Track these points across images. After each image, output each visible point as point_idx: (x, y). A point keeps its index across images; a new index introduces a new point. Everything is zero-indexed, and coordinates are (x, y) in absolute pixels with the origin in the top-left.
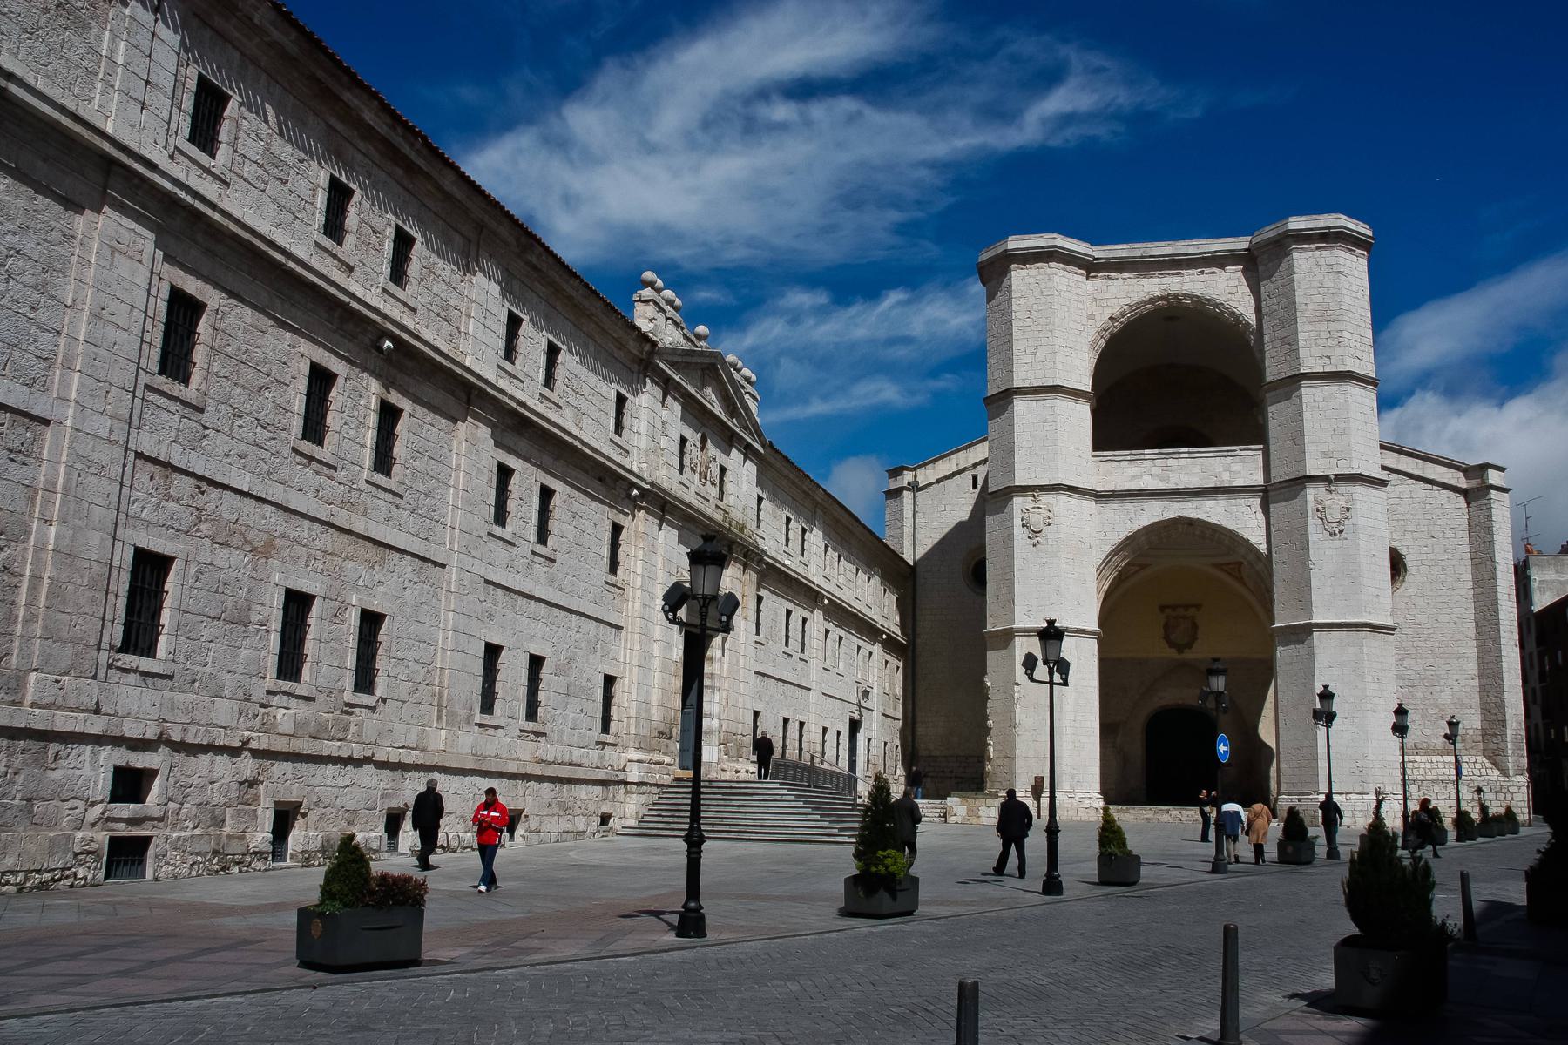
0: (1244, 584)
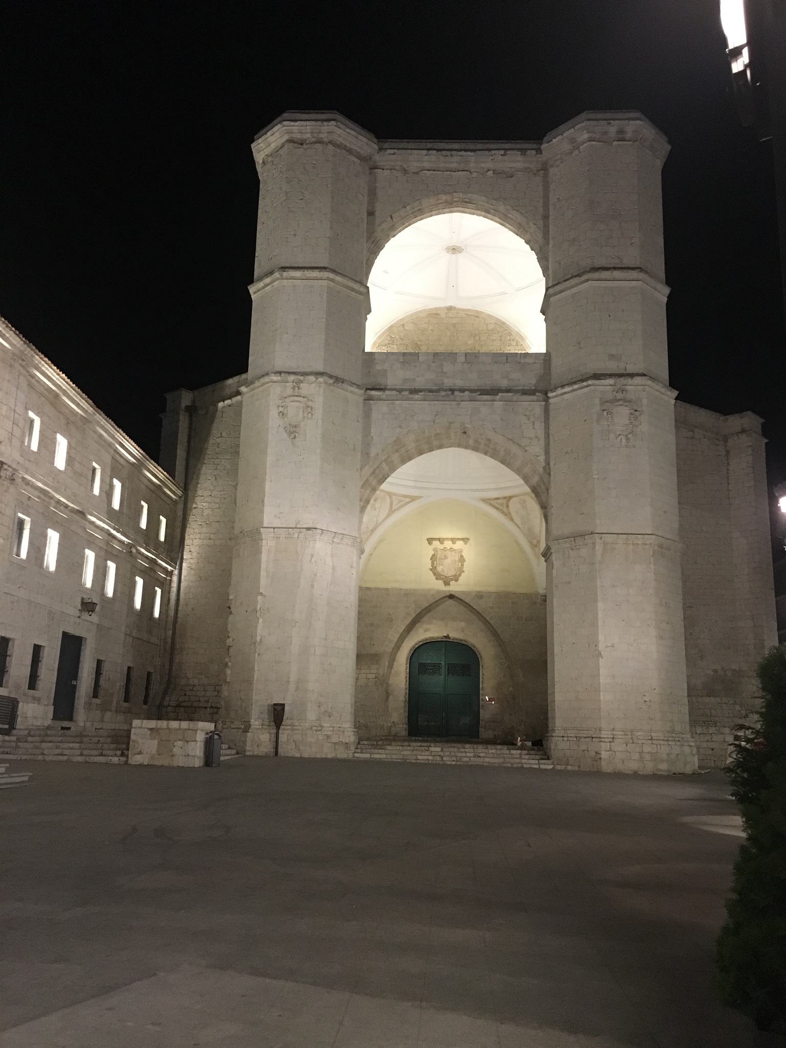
0: (512, 520)
